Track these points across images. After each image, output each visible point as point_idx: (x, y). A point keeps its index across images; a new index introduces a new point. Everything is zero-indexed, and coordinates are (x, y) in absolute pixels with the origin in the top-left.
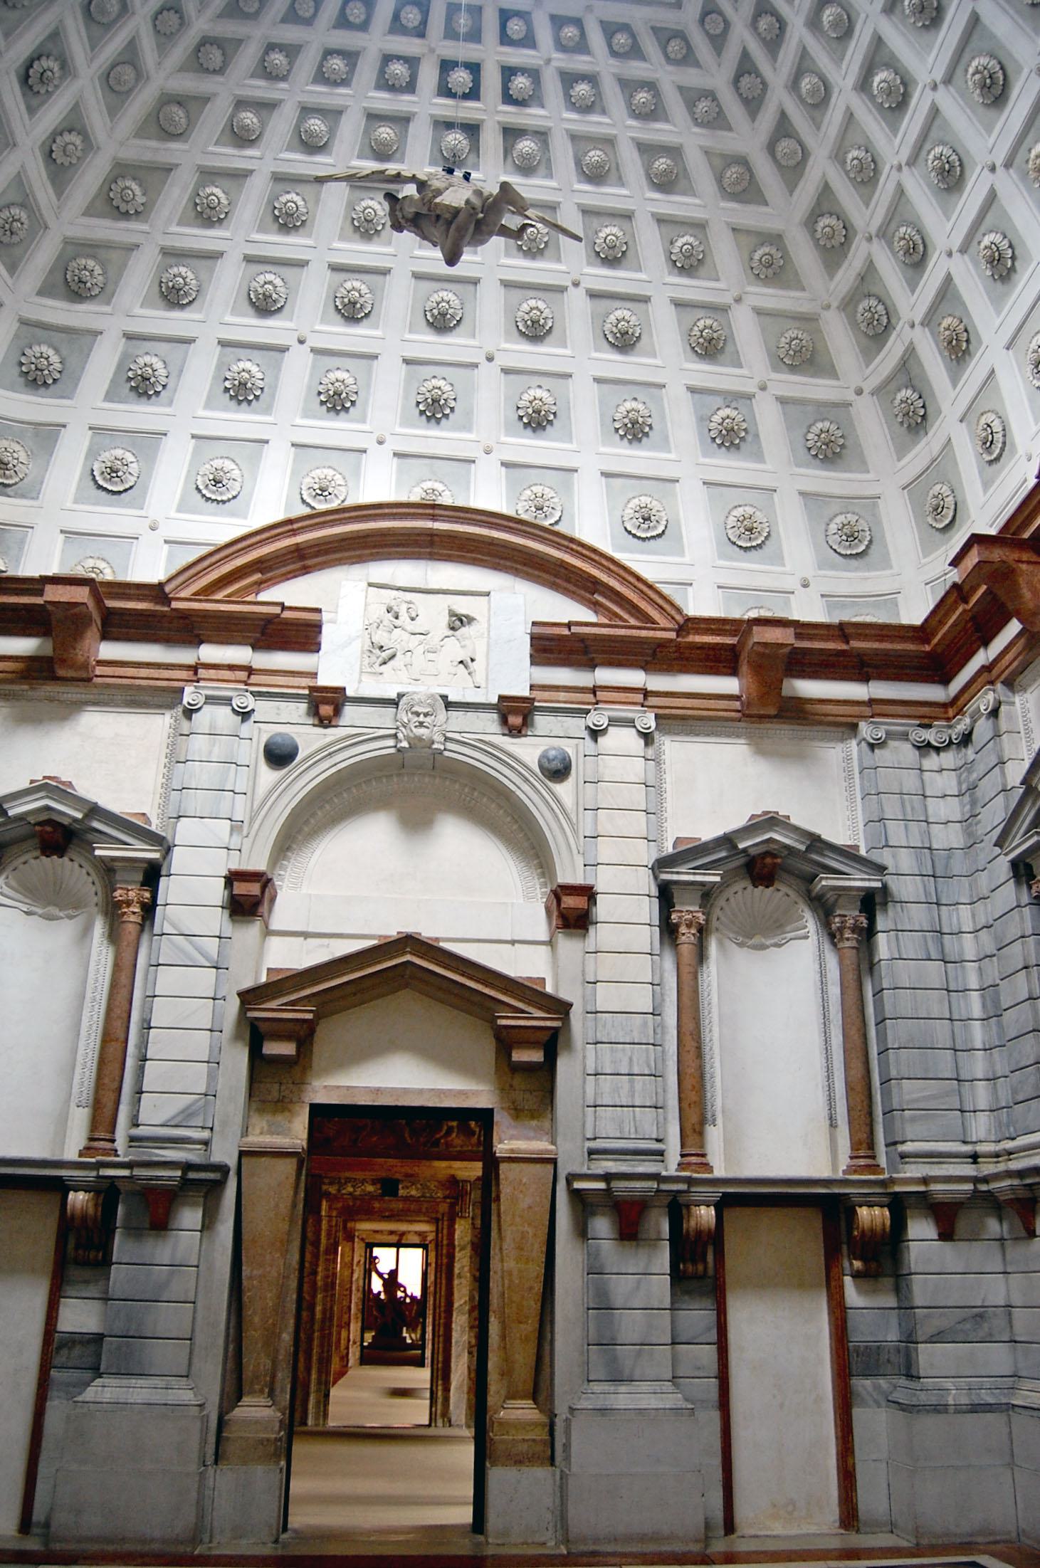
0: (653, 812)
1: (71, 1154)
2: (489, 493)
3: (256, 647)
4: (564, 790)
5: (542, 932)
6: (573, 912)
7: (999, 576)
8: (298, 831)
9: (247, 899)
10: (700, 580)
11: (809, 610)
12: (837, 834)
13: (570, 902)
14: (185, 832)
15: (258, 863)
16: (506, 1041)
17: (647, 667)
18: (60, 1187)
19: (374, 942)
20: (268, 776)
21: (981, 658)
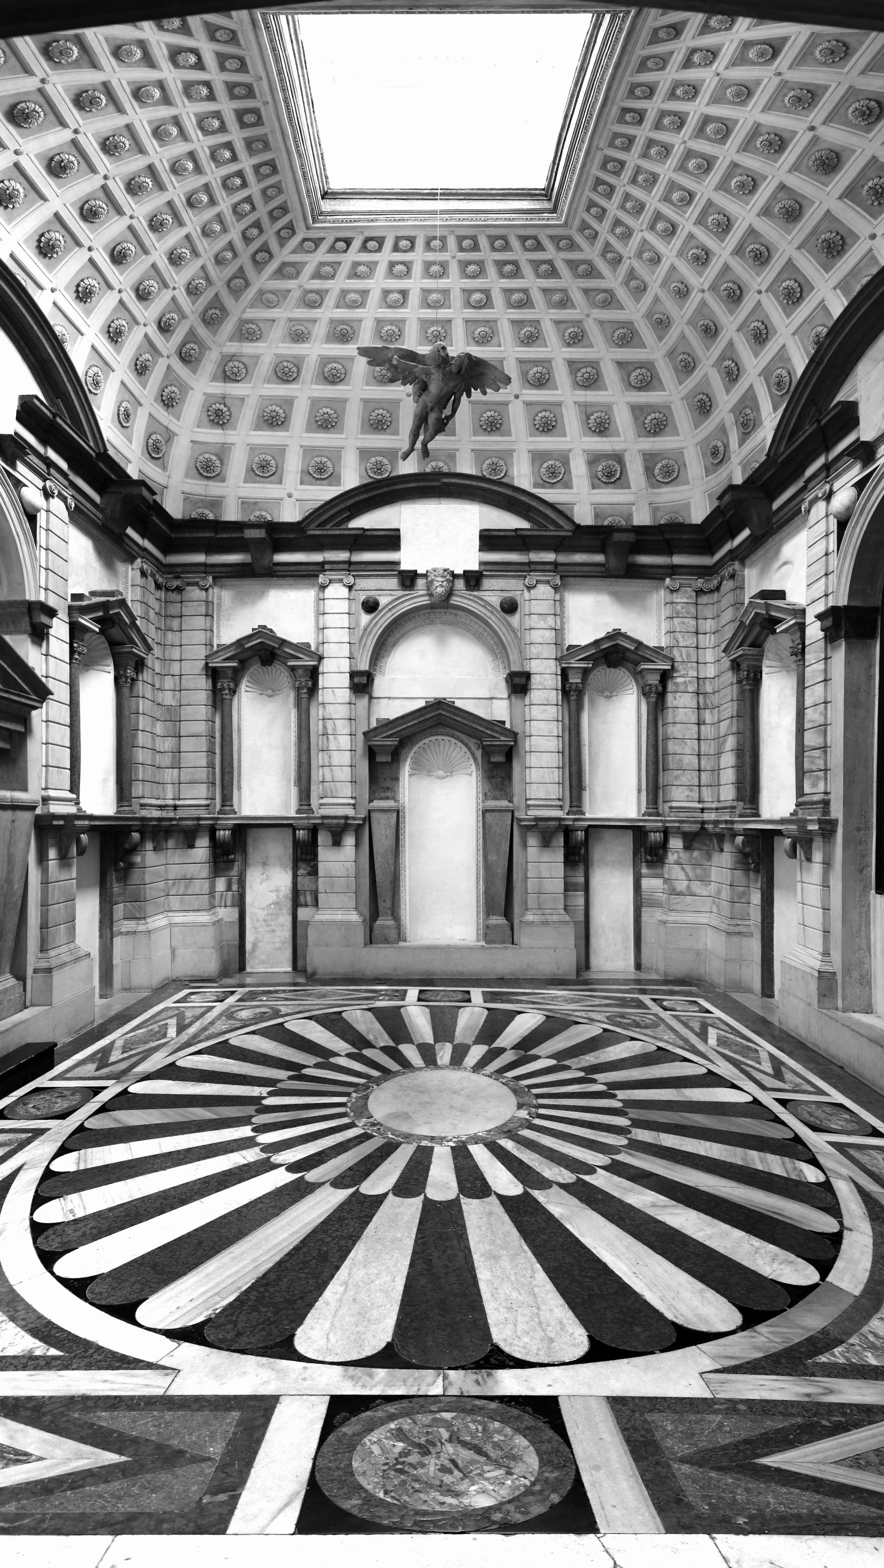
0: (559, 632)
1: (293, 814)
2: (466, 466)
3: (351, 551)
4: (515, 620)
5: (506, 695)
6: (519, 684)
7: (736, 504)
8: (382, 647)
9: (362, 684)
10: (584, 502)
11: (642, 518)
12: (651, 643)
13: (517, 680)
14: (328, 650)
15: (364, 666)
16: (487, 752)
17: (557, 549)
18: (290, 825)
19: (421, 704)
20: (365, 618)
21: (728, 547)
